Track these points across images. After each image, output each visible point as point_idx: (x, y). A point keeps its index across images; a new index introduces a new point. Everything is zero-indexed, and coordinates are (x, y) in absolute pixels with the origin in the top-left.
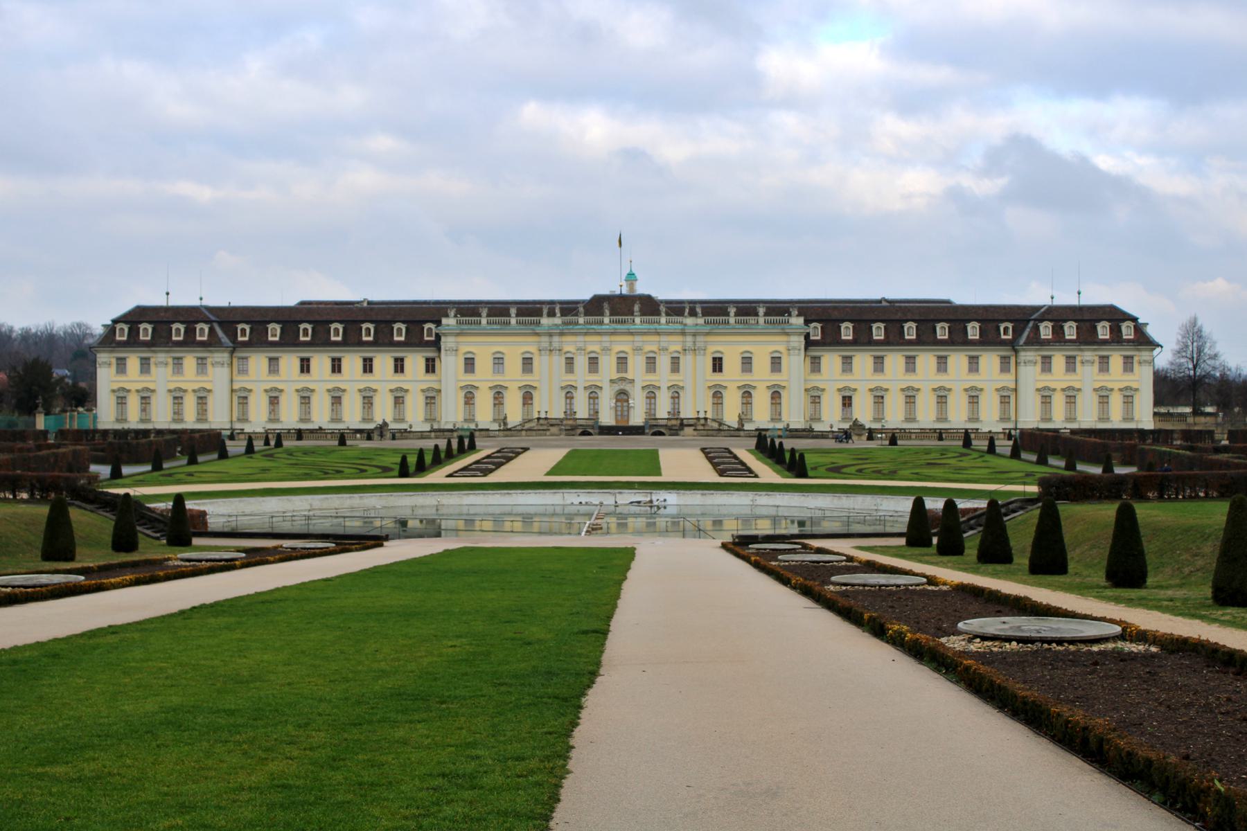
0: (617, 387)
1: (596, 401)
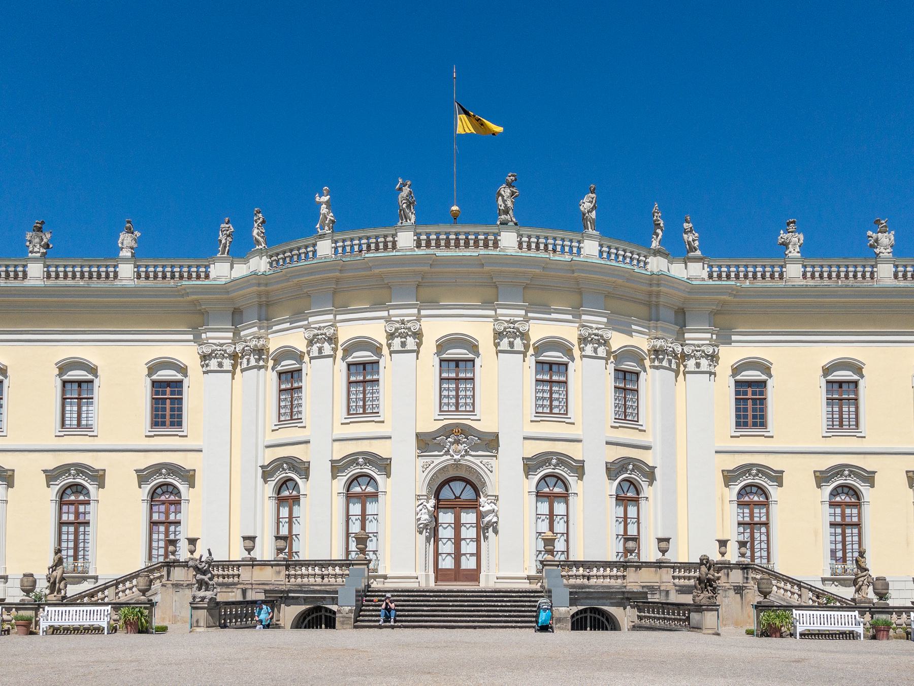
0: (439, 460)
1: (371, 508)
